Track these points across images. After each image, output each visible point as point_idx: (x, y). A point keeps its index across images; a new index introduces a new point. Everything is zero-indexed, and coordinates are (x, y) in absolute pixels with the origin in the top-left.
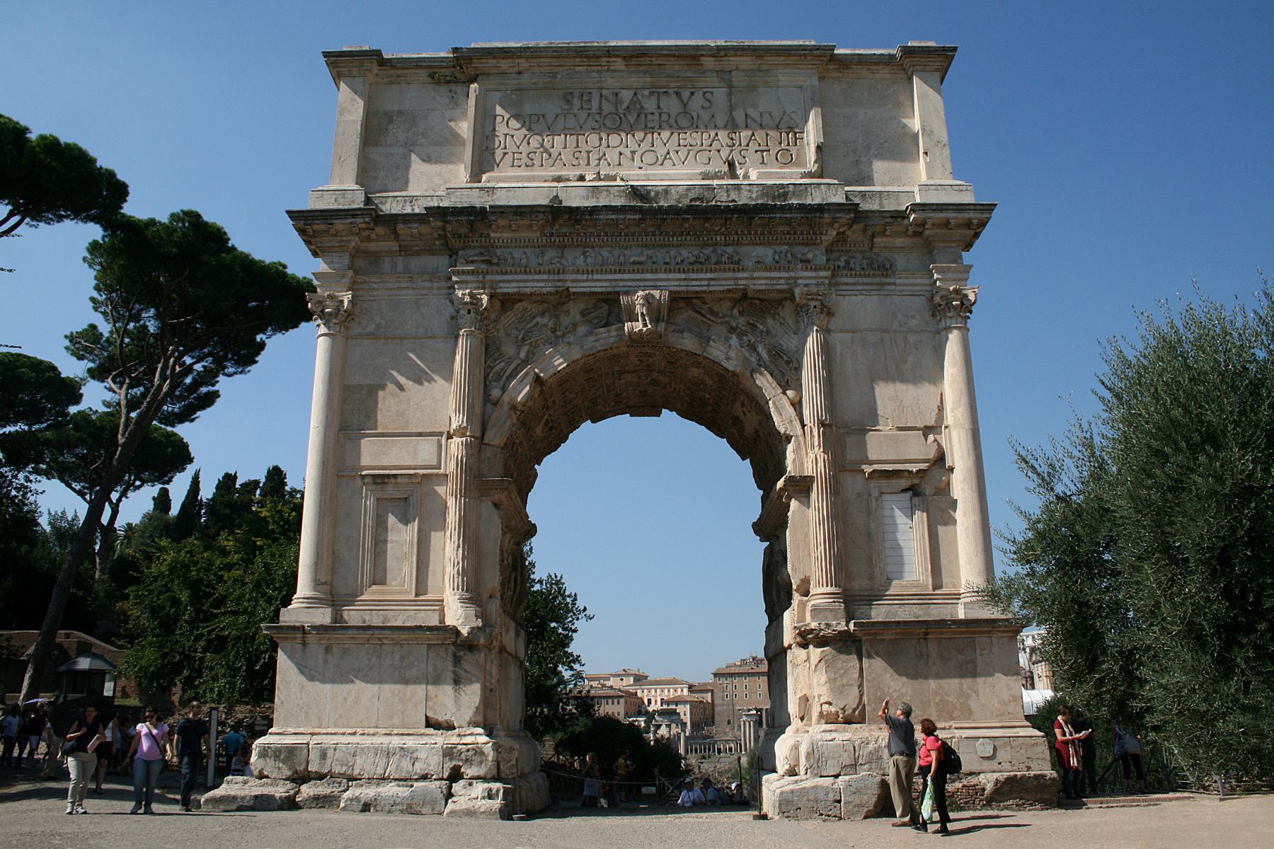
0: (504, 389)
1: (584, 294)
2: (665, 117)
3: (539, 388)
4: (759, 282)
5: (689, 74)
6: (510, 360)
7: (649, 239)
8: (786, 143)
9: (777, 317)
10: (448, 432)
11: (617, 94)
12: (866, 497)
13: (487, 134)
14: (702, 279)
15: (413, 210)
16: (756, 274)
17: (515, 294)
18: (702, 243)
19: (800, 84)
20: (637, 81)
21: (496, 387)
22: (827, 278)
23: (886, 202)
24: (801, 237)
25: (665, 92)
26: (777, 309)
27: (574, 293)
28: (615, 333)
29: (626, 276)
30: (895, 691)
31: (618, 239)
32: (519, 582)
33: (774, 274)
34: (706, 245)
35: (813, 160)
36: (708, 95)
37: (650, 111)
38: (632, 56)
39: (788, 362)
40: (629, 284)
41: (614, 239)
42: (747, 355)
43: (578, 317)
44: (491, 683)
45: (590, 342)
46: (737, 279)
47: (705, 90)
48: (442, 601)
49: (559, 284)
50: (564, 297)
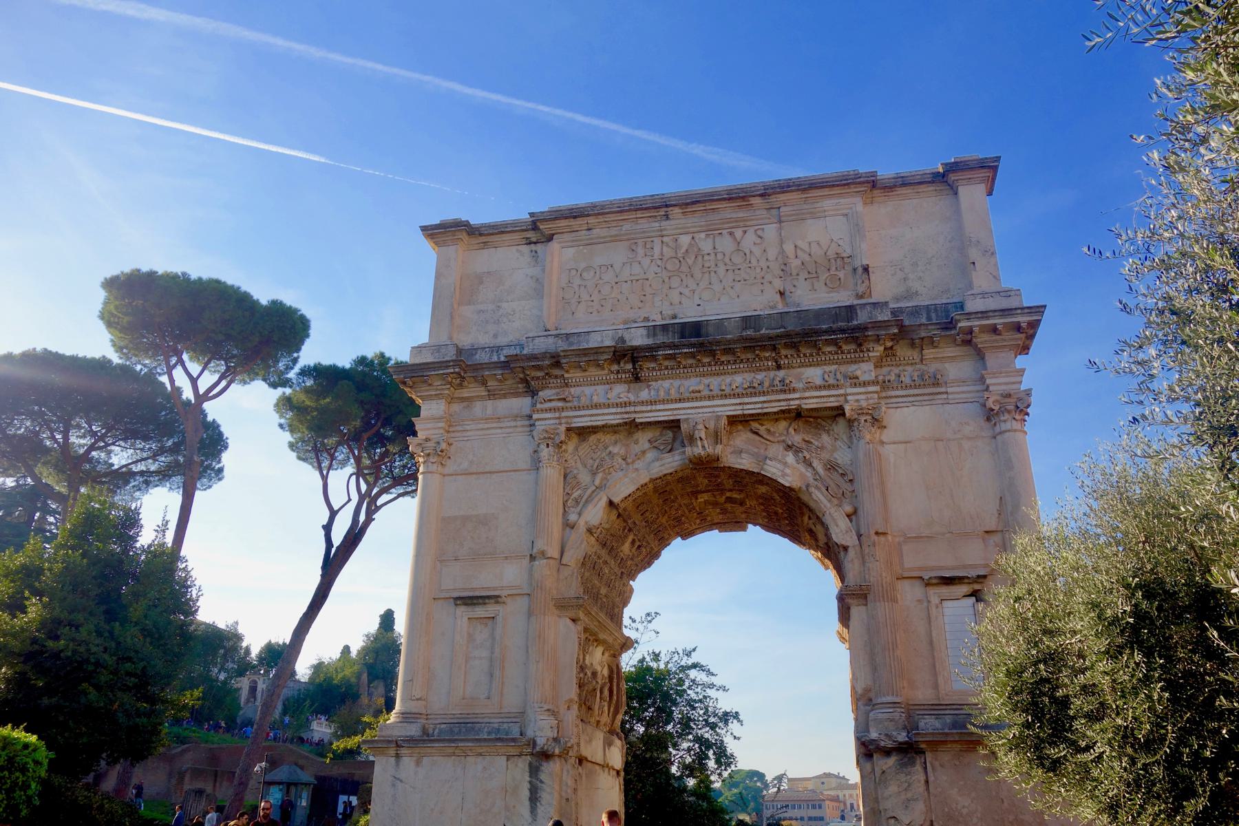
0: (580, 514)
1: (650, 423)
2: (720, 256)
3: (615, 512)
4: (811, 402)
5: (741, 215)
7: (705, 369)
8: (834, 268)
9: (831, 432)
10: (531, 555)
12: (925, 604)
14: (756, 403)
15: (499, 358)
16: (807, 394)
17: (589, 427)
18: (755, 369)
19: (845, 212)
22: (876, 392)
23: (933, 315)
24: (849, 356)
25: (720, 234)
26: (831, 425)
27: (641, 423)
28: (680, 457)
30: (964, 807)
31: (678, 372)
32: (615, 692)
34: (759, 370)
35: (860, 282)
36: (759, 233)
37: (706, 252)
38: (687, 204)
39: (842, 475)
40: (689, 411)
41: (674, 372)
43: (647, 445)
44: (566, 792)
46: (789, 400)
47: (757, 227)
48: (524, 713)
49: (626, 416)
50: (632, 427)
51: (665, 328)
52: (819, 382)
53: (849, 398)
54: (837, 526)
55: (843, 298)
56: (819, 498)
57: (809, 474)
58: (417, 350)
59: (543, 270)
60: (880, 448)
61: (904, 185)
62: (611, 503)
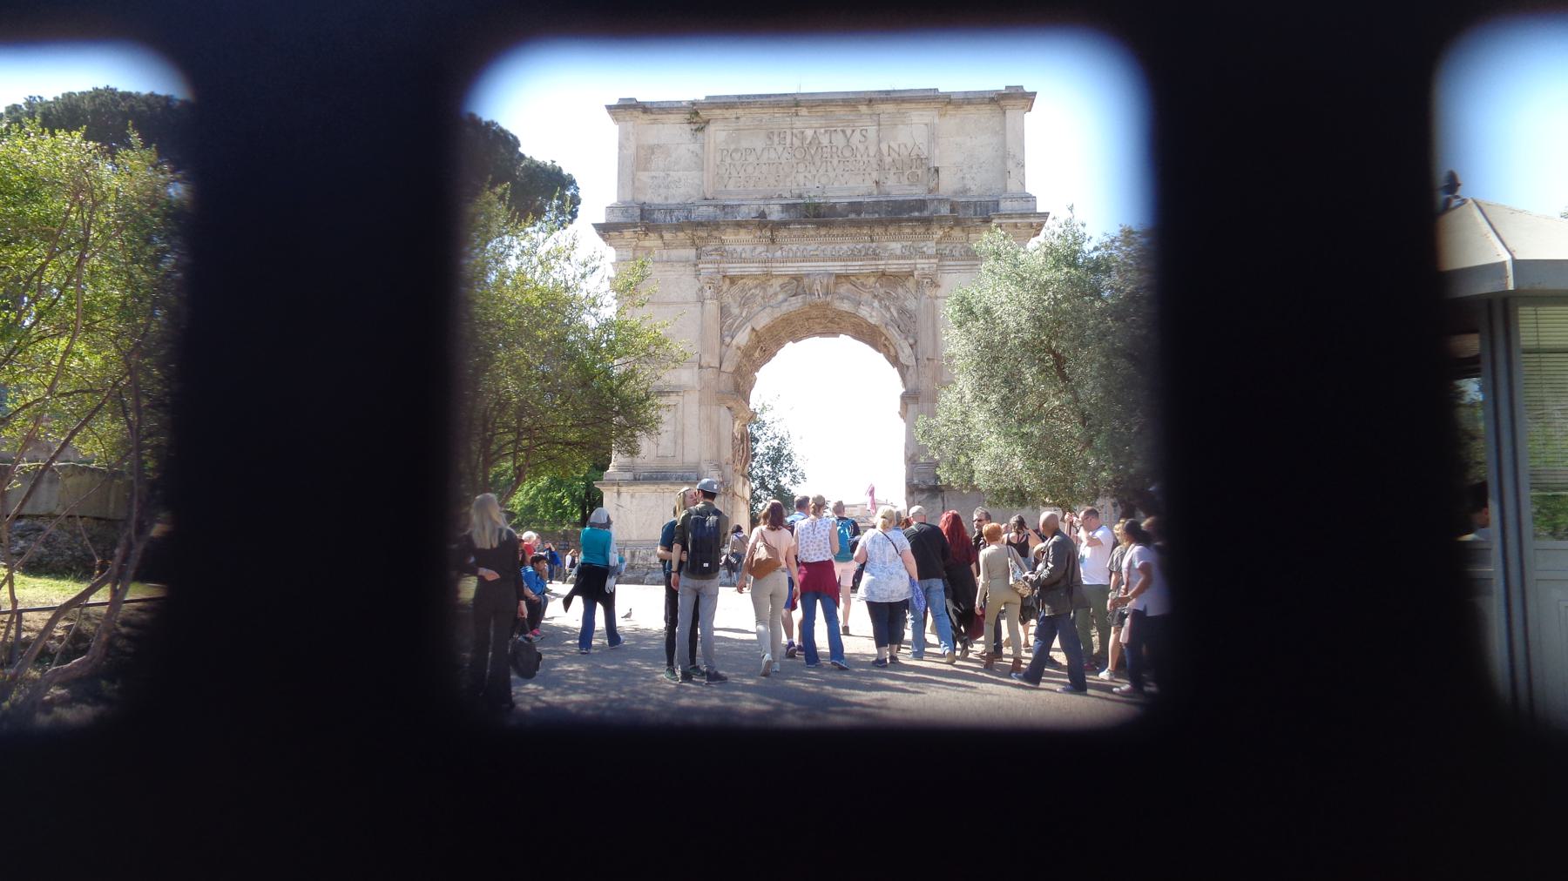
2: (834, 149)
4: (893, 266)
5: (851, 117)
6: (736, 318)
11: (803, 133)
13: (718, 163)
16: (890, 262)
20: (815, 123)
21: (728, 336)
25: (835, 130)
29: (808, 264)
33: (901, 262)
35: (931, 179)
36: (864, 132)
42: (884, 313)
43: (778, 289)
45: (785, 308)
51: (794, 205)
52: (898, 252)
53: (918, 266)
54: (903, 352)
55: (918, 192)
56: (893, 333)
57: (888, 316)
58: (611, 209)
59: (703, 147)
60: (935, 301)
61: (969, 104)
62: (753, 329)
